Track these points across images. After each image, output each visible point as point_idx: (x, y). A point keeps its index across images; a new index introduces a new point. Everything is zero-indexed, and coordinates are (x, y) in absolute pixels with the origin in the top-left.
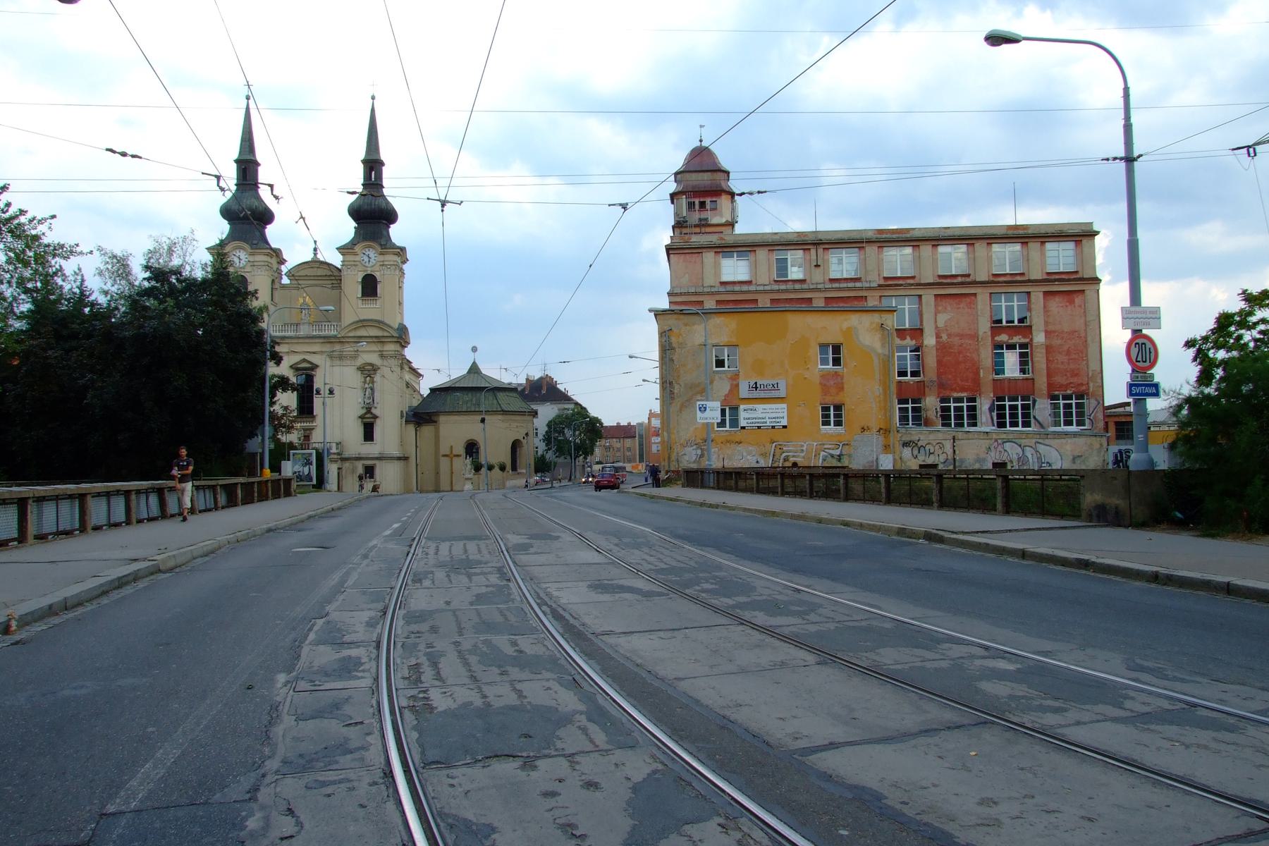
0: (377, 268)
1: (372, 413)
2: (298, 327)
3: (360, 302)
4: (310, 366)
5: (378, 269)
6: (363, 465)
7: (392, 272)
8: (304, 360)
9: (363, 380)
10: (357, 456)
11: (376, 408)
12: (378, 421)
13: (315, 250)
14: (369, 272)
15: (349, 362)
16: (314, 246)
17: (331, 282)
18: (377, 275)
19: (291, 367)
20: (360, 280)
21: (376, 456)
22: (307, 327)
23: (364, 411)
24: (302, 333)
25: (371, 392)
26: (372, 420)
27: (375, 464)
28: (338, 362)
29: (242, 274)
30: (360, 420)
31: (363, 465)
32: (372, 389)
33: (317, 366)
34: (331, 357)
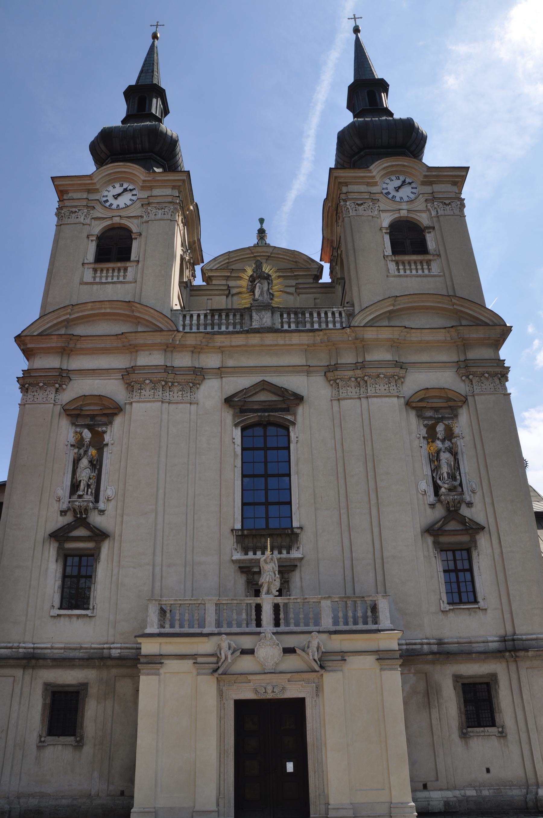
0: (420, 205)
1: (462, 520)
2: (247, 317)
3: (392, 266)
4: (275, 398)
5: (422, 207)
6: (457, 678)
7: (457, 212)
8: (264, 386)
9: (424, 432)
10: (435, 648)
11: (470, 505)
12: (483, 541)
13: (262, 232)
14: (404, 213)
15: (382, 388)
16: (259, 226)
17: (293, 282)
18: (424, 219)
19: (229, 401)
20: (386, 224)
21: (494, 646)
22: (269, 314)
23: (440, 512)
24: (255, 325)
25: (452, 459)
26: (465, 538)
27: (494, 677)
28: (352, 391)
29: (124, 222)
30: (430, 540)
31: (457, 678)
32: (455, 454)
33: (299, 399)
34: (334, 383)
